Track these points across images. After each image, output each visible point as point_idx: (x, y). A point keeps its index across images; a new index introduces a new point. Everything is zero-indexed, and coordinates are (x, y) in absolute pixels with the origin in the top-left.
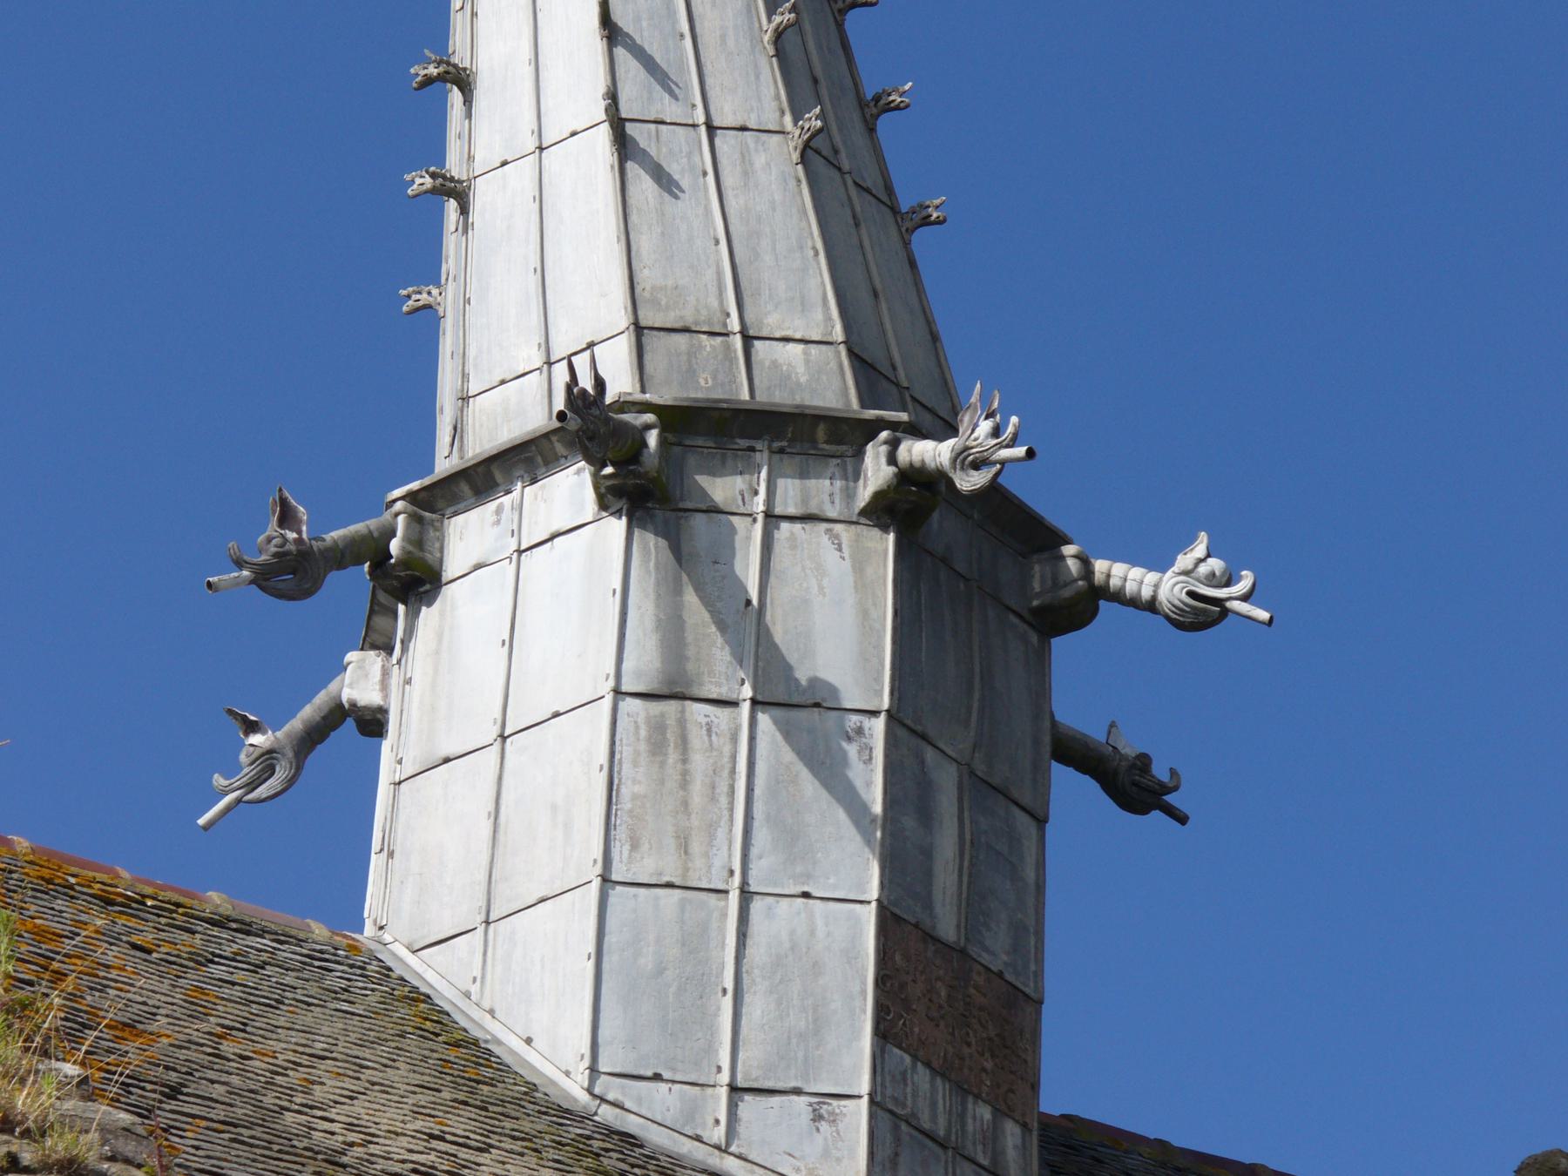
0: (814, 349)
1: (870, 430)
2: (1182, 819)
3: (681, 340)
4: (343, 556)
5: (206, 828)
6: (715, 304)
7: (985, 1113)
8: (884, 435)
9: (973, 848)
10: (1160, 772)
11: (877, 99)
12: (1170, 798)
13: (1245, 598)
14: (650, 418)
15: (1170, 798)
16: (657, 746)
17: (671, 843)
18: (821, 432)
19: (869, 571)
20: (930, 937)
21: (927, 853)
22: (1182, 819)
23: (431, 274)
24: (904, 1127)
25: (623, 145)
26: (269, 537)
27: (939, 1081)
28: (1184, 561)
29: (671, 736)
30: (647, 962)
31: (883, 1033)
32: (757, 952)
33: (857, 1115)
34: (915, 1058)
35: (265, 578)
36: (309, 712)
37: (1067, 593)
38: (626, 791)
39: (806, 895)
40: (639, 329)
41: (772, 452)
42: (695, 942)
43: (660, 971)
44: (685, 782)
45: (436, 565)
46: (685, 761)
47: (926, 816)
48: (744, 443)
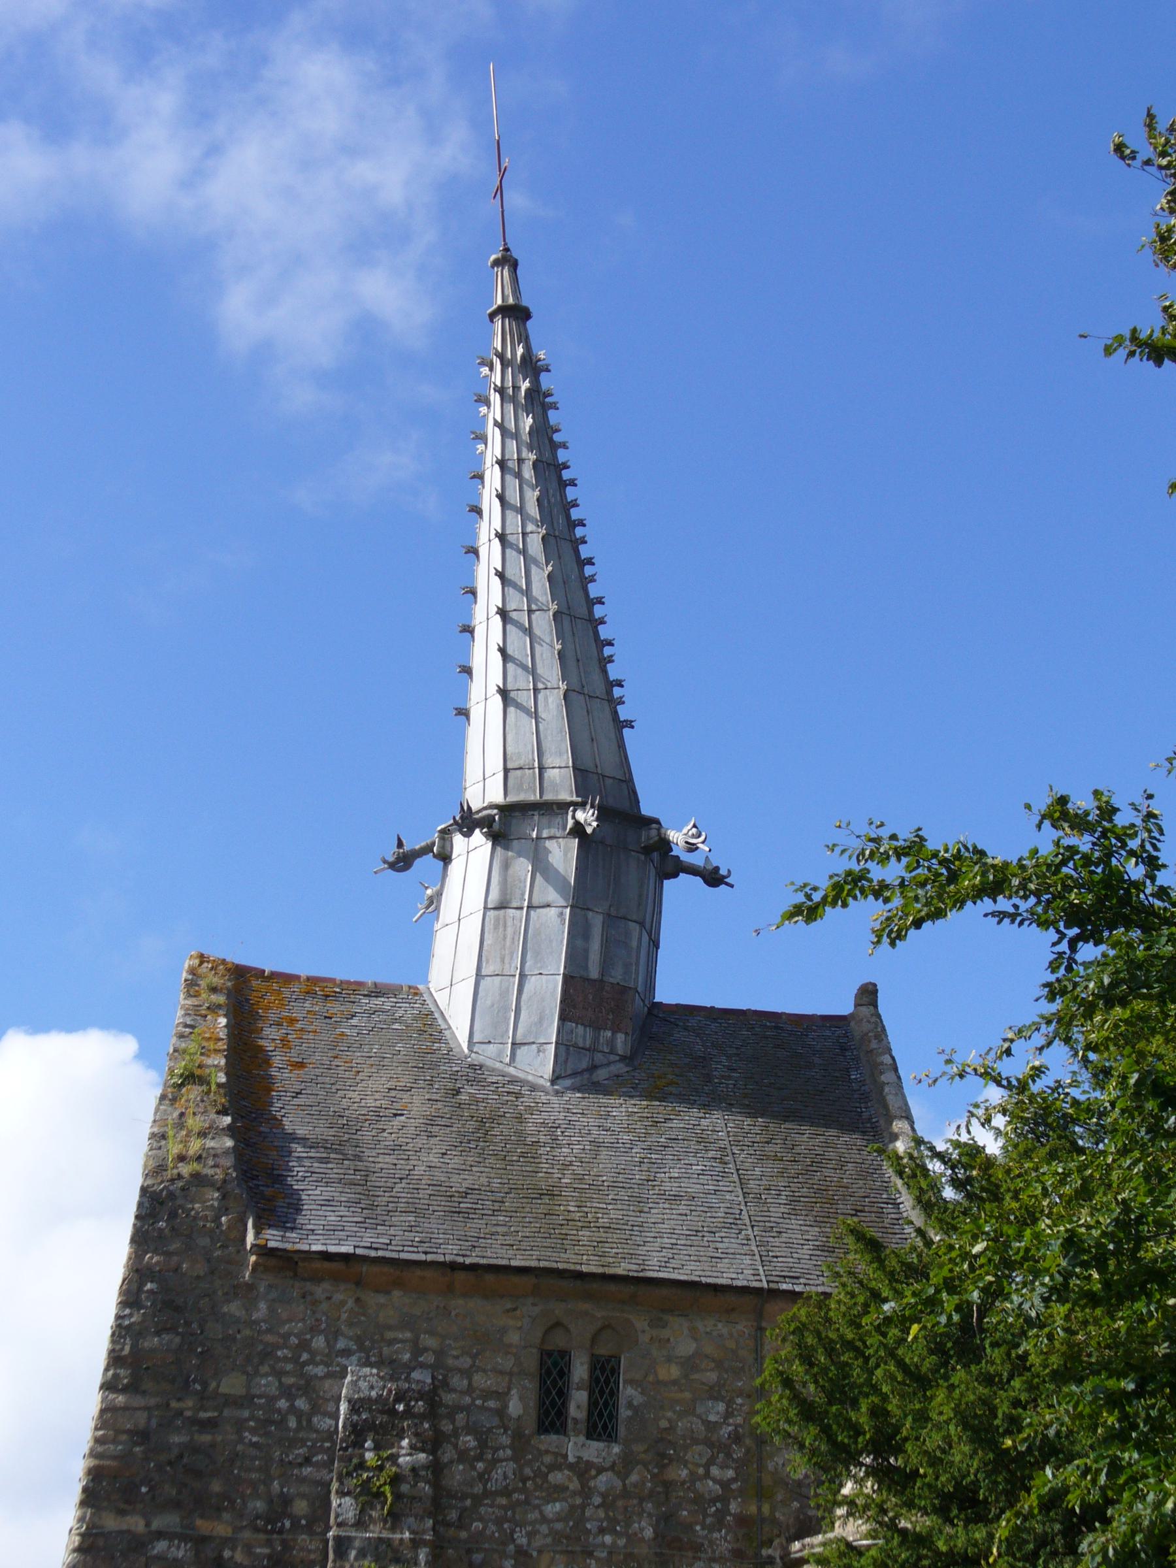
0: (562, 770)
2: (732, 886)
3: (519, 772)
5: (416, 921)
6: (531, 757)
7: (609, 1034)
8: (571, 808)
9: (606, 943)
10: (723, 872)
11: (609, 657)
12: (727, 880)
13: (703, 842)
14: (495, 811)
15: (727, 880)
16: (496, 927)
17: (498, 960)
18: (555, 807)
19: (569, 855)
21: (586, 951)
22: (732, 886)
24: (571, 1048)
26: (391, 853)
27: (588, 1029)
28: (685, 831)
29: (501, 923)
30: (489, 1003)
31: (563, 1018)
32: (524, 997)
33: (552, 1049)
34: (577, 1024)
35: (392, 866)
37: (651, 842)
38: (486, 943)
39: (541, 974)
40: (506, 771)
41: (539, 815)
43: (493, 1005)
44: (505, 938)
45: (448, 854)
46: (505, 930)
48: (530, 813)
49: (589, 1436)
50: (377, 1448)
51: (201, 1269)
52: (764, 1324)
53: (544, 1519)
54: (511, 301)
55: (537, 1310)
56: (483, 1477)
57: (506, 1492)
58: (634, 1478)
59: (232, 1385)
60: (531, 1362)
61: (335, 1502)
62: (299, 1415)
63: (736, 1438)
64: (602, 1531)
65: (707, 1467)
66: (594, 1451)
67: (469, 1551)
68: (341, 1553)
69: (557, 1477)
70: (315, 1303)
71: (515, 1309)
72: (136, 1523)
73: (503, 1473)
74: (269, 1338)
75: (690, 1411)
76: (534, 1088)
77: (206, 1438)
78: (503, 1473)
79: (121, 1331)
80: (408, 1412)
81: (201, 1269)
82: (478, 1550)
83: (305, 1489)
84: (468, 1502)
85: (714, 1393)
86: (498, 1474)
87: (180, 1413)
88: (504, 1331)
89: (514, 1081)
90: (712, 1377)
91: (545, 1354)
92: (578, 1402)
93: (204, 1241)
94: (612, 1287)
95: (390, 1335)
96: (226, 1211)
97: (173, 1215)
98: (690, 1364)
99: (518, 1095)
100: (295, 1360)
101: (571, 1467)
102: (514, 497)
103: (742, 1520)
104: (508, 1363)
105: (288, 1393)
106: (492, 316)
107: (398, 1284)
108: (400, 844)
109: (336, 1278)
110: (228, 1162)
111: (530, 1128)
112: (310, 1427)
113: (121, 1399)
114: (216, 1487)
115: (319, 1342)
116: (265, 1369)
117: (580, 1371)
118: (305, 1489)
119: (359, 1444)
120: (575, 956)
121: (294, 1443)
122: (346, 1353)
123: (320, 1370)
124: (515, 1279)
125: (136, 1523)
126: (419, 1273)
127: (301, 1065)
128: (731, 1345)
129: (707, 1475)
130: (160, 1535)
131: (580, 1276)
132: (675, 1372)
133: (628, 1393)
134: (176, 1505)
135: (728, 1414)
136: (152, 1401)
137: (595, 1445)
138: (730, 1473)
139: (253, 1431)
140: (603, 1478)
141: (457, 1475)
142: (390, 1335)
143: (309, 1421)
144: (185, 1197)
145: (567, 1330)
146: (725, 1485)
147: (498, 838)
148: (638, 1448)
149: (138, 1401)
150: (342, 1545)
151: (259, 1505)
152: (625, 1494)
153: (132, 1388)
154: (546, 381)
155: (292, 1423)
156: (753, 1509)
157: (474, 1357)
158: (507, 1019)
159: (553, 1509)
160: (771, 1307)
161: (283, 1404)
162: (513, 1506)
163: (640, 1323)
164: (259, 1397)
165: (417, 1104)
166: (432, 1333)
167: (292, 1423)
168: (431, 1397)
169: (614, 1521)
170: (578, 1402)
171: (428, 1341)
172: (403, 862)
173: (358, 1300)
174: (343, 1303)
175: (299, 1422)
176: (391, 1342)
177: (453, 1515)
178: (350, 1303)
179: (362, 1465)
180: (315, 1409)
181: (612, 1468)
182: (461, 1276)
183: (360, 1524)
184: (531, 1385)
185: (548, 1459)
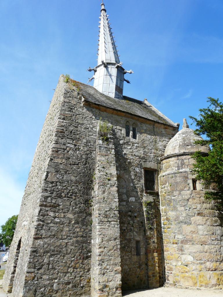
1: (116, 64)
4: (92, 70)
9: (120, 83)
16: (106, 77)
20: (118, 86)
23: (97, 59)
25: (105, 52)
26: (89, 69)
31: (116, 90)
33: (114, 93)
36: (92, 78)
38: (104, 79)
47: (118, 81)
52: (154, 127)
55: (125, 119)
64: (136, 152)
67: (118, 152)
71: (122, 118)
82: (119, 152)
84: (117, 145)
88: (120, 121)
89: (109, 97)
94: (136, 117)
101: (131, 142)
106: (101, 11)
107: (105, 111)
109: (96, 108)
113: (62, 121)
118: (92, 139)
120: (117, 83)
123: (94, 122)
126: (109, 109)
130: (69, 143)
138: (152, 146)
143: (92, 129)
144: (72, 92)
145: (129, 122)
153: (64, 119)
157: (117, 124)
160: (156, 124)
163: (139, 124)
164: (85, 124)
167: (90, 129)
171: (110, 120)
172: (90, 70)
173: (99, 112)
174: (97, 112)
175: (91, 129)
178: (98, 112)
182: (115, 111)
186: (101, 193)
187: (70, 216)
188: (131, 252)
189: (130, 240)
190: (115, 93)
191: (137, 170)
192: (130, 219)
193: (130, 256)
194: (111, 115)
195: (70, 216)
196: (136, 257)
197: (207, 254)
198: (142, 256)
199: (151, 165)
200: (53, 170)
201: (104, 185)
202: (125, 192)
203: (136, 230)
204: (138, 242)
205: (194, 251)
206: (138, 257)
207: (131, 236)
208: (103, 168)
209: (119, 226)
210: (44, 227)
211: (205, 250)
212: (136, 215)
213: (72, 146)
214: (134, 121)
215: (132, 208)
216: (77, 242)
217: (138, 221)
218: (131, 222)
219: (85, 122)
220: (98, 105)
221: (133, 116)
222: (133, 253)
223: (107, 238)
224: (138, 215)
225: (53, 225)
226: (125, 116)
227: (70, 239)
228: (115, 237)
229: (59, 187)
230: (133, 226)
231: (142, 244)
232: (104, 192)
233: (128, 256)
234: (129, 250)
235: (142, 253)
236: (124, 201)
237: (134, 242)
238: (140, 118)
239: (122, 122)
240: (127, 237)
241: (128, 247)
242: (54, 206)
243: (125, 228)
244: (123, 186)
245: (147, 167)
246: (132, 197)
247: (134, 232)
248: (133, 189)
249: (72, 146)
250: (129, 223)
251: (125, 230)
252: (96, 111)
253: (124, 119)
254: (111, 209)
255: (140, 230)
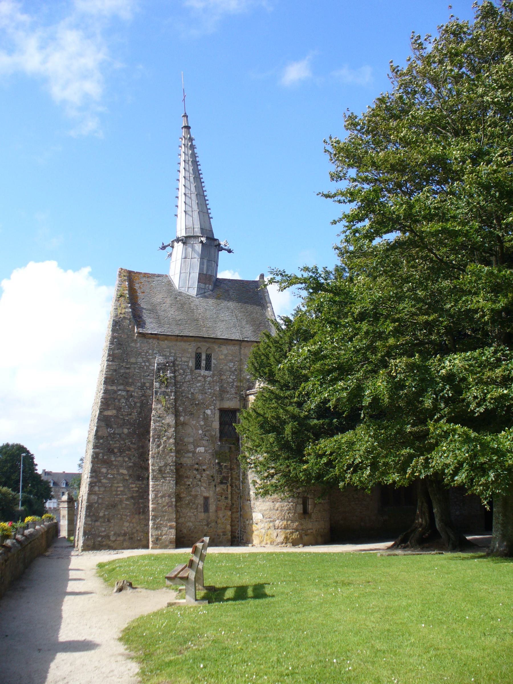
9: (207, 266)
31: (198, 282)
35: (161, 249)
40: (186, 229)
42: (186, 277)
47: (203, 265)
49: (206, 370)
50: (163, 373)
51: (126, 336)
53: (197, 387)
54: (186, 125)
55: (195, 345)
56: (184, 378)
57: (189, 381)
58: (215, 378)
59: (133, 360)
60: (194, 355)
61: (155, 384)
62: (147, 366)
63: (236, 370)
64: (209, 389)
65: (230, 376)
66: (207, 373)
68: (156, 394)
69: (199, 378)
70: (150, 343)
72: (114, 388)
73: (188, 377)
74: (140, 351)
75: (226, 365)
76: (192, 297)
77: (128, 371)
78: (188, 377)
79: (110, 349)
80: (169, 366)
81: (126, 336)
83: (148, 381)
85: (231, 361)
86: (187, 378)
87: (122, 366)
88: (188, 349)
89: (188, 295)
90: (231, 358)
91: (197, 353)
92: (203, 363)
93: (126, 331)
94: (210, 340)
95: (165, 350)
96: (130, 324)
97: (119, 326)
98: (226, 355)
99: (189, 299)
100: (145, 355)
101: (202, 376)
102: (187, 168)
103: (237, 387)
104: (189, 356)
105: (144, 362)
106: (182, 128)
107: (166, 339)
108: (163, 244)
109: (154, 338)
110: (130, 314)
111: (192, 306)
112: (149, 369)
113: (110, 363)
114: (130, 381)
115: (150, 351)
116: (139, 357)
117: (204, 357)
118: (148, 381)
119: (159, 372)
120: (201, 269)
121: (146, 372)
122: (156, 353)
123: (151, 357)
124: (191, 338)
125: (114, 388)
127: (143, 292)
128: (235, 351)
129: (230, 378)
130: (120, 390)
131: (204, 338)
132: (223, 357)
133: (213, 361)
134: (123, 384)
135: (234, 366)
136: (117, 364)
137: (207, 372)
138: (234, 377)
139: (138, 369)
140: (209, 378)
141: (179, 378)
142: (165, 350)
146: (233, 380)
147: (184, 243)
148: (216, 372)
149: (114, 363)
150: (156, 392)
151: (139, 384)
152: (213, 382)
154: (194, 143)
155: (145, 368)
156: (239, 384)
158: (186, 283)
159: (199, 384)
160: (243, 344)
161: (143, 364)
162: (190, 384)
163: (216, 347)
165: (168, 301)
166: (173, 349)
167: (145, 368)
168: (174, 363)
169: (211, 387)
170: (203, 363)
171: (173, 351)
172: (164, 248)
176: (165, 351)
177: (178, 386)
179: (160, 376)
180: (150, 365)
181: (210, 376)
182: (179, 338)
183: (160, 388)
184: (194, 360)
185: (197, 375)
186: (155, 447)
187: (125, 472)
188: (196, 508)
189: (197, 496)
190: (199, 288)
191: (209, 412)
192: (196, 473)
193: (195, 513)
194: (174, 343)
195: (125, 472)
196: (203, 514)
197: (278, 512)
198: (211, 514)
199: (230, 404)
200: (103, 424)
201: (159, 437)
202: (192, 441)
203: (204, 485)
204: (206, 499)
205: (264, 509)
206: (206, 514)
207: (198, 492)
208: (159, 417)
209: (174, 482)
210: (97, 484)
211: (276, 508)
212: (204, 467)
213: (124, 393)
214: (208, 345)
215: (199, 460)
216: (132, 497)
217: (208, 475)
218: (198, 476)
219: (140, 360)
220: (156, 334)
221: (207, 339)
222: (199, 510)
223: (160, 495)
224: (207, 468)
225: (107, 481)
226: (194, 341)
227: (125, 495)
228: (169, 493)
229: (111, 442)
230: (200, 481)
231: (211, 501)
232: (159, 446)
233: (193, 513)
234: (194, 506)
235: (211, 511)
236: (190, 452)
237: (202, 498)
238: (216, 340)
239: (190, 350)
240: (193, 493)
241: (194, 503)
242: (107, 463)
243: (190, 483)
244: (189, 434)
245: (225, 407)
246: (201, 447)
247: (202, 488)
248: (202, 438)
249: (124, 393)
250: (195, 478)
251: (189, 485)
252: (154, 342)
253: (193, 344)
254: (166, 465)
255: (209, 485)
